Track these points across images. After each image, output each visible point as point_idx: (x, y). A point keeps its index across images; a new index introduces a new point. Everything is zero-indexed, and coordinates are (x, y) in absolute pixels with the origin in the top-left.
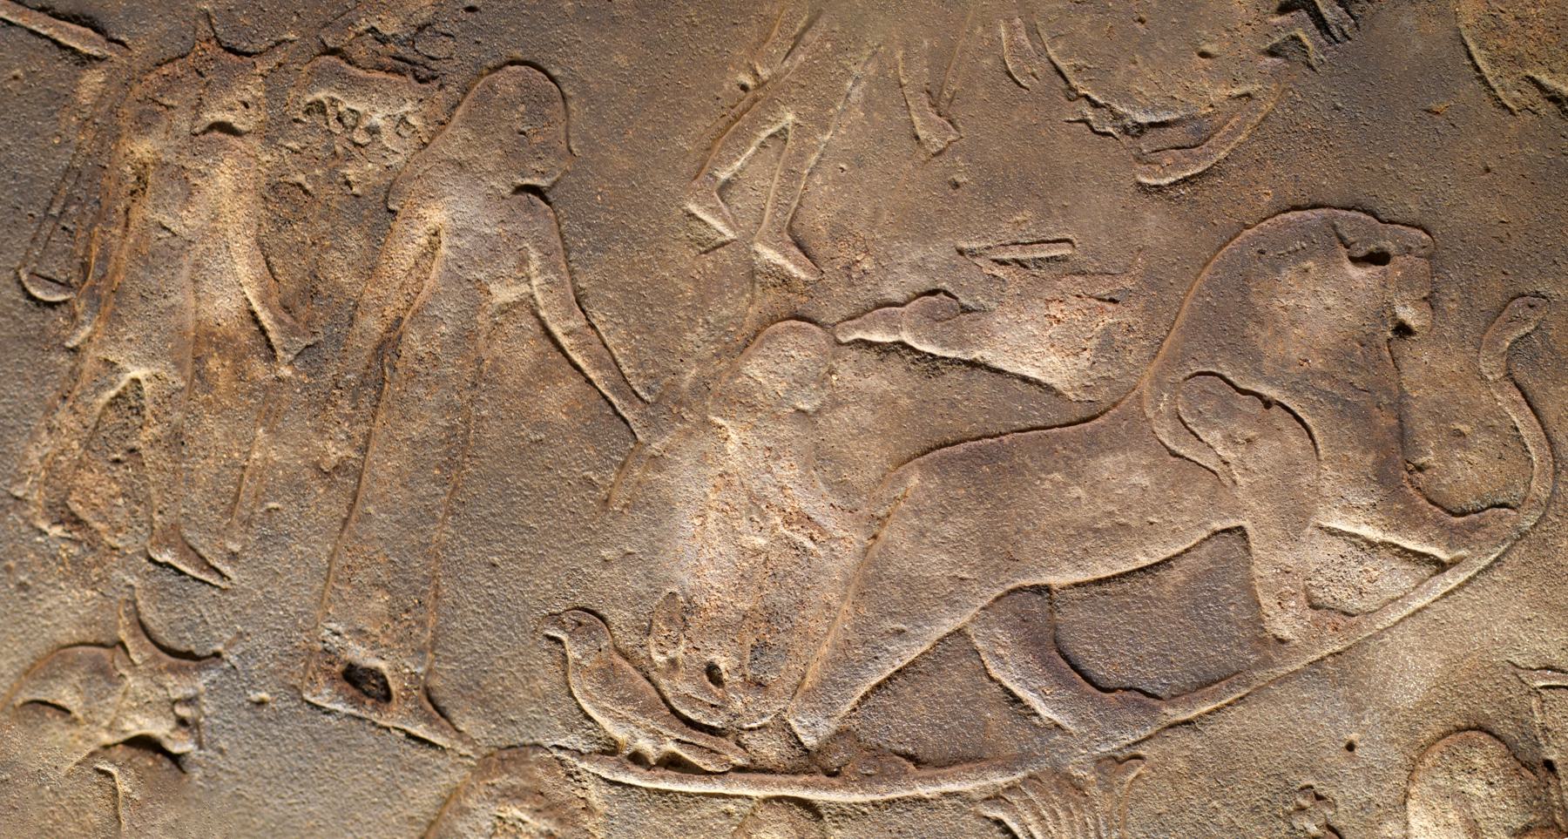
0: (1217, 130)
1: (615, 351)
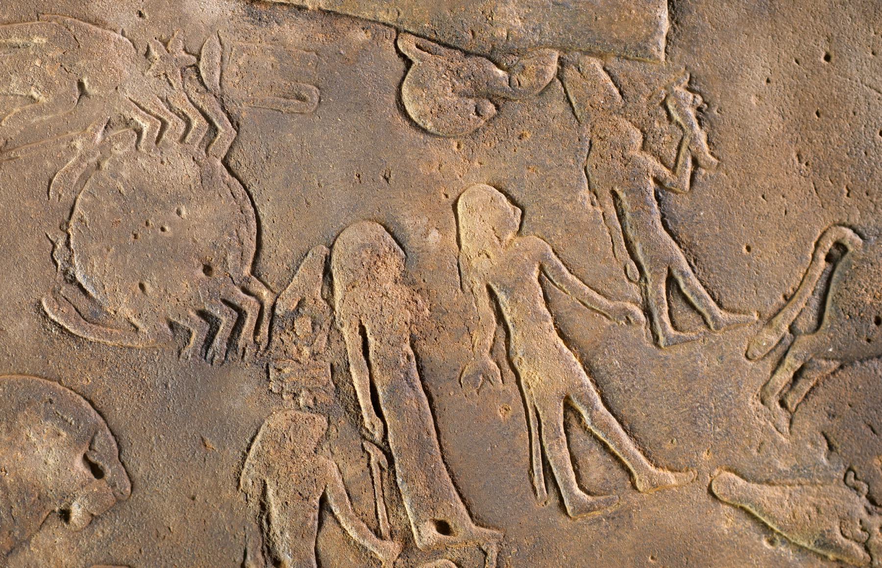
0: (104, 325)
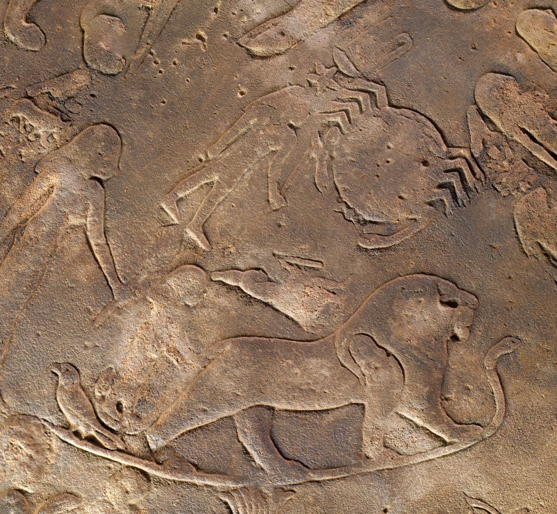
0: (398, 231)
1: (114, 258)
